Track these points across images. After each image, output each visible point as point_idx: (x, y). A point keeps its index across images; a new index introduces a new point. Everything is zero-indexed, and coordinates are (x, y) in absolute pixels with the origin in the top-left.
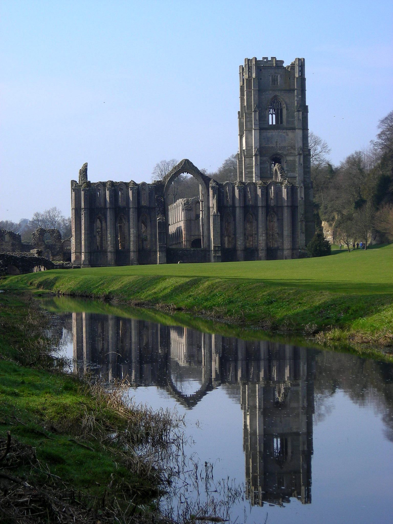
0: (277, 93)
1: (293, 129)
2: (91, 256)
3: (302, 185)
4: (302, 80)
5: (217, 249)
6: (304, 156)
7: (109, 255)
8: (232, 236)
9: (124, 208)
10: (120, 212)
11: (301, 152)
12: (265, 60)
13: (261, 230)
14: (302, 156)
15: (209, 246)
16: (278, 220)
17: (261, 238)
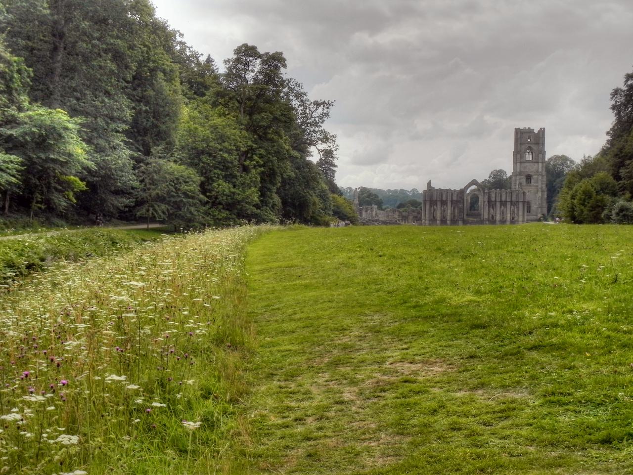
0: (531, 145)
1: (538, 162)
7: (438, 222)
10: (444, 203)
13: (508, 212)
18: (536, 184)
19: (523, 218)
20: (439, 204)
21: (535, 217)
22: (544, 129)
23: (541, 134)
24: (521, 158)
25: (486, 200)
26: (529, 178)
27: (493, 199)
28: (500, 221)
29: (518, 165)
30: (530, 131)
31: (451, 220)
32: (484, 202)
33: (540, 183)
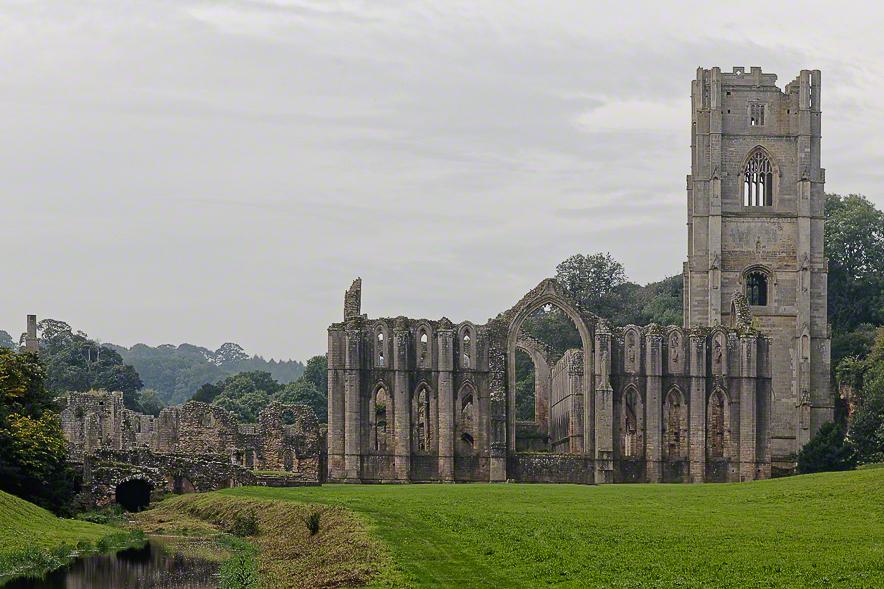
2: (362, 463)
3: (806, 332)
4: (815, 113)
5: (605, 457)
6: (812, 273)
7: (397, 461)
8: (640, 433)
9: (429, 372)
10: (418, 379)
11: (805, 266)
12: (739, 73)
13: (697, 422)
14: (809, 272)
15: (593, 451)
16: (729, 404)
17: (694, 440)
18: (790, 310)
19: (760, 448)
20: (399, 383)
21: (785, 443)
22: (817, 74)
23: (804, 93)
24: (724, 195)
25: (602, 367)
26: (758, 284)
27: (631, 368)
28: (664, 460)
29: (715, 223)
30: (763, 82)
31: (457, 459)
32: (593, 376)
33: (804, 301)
